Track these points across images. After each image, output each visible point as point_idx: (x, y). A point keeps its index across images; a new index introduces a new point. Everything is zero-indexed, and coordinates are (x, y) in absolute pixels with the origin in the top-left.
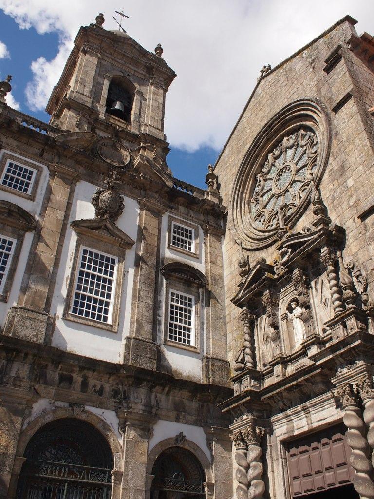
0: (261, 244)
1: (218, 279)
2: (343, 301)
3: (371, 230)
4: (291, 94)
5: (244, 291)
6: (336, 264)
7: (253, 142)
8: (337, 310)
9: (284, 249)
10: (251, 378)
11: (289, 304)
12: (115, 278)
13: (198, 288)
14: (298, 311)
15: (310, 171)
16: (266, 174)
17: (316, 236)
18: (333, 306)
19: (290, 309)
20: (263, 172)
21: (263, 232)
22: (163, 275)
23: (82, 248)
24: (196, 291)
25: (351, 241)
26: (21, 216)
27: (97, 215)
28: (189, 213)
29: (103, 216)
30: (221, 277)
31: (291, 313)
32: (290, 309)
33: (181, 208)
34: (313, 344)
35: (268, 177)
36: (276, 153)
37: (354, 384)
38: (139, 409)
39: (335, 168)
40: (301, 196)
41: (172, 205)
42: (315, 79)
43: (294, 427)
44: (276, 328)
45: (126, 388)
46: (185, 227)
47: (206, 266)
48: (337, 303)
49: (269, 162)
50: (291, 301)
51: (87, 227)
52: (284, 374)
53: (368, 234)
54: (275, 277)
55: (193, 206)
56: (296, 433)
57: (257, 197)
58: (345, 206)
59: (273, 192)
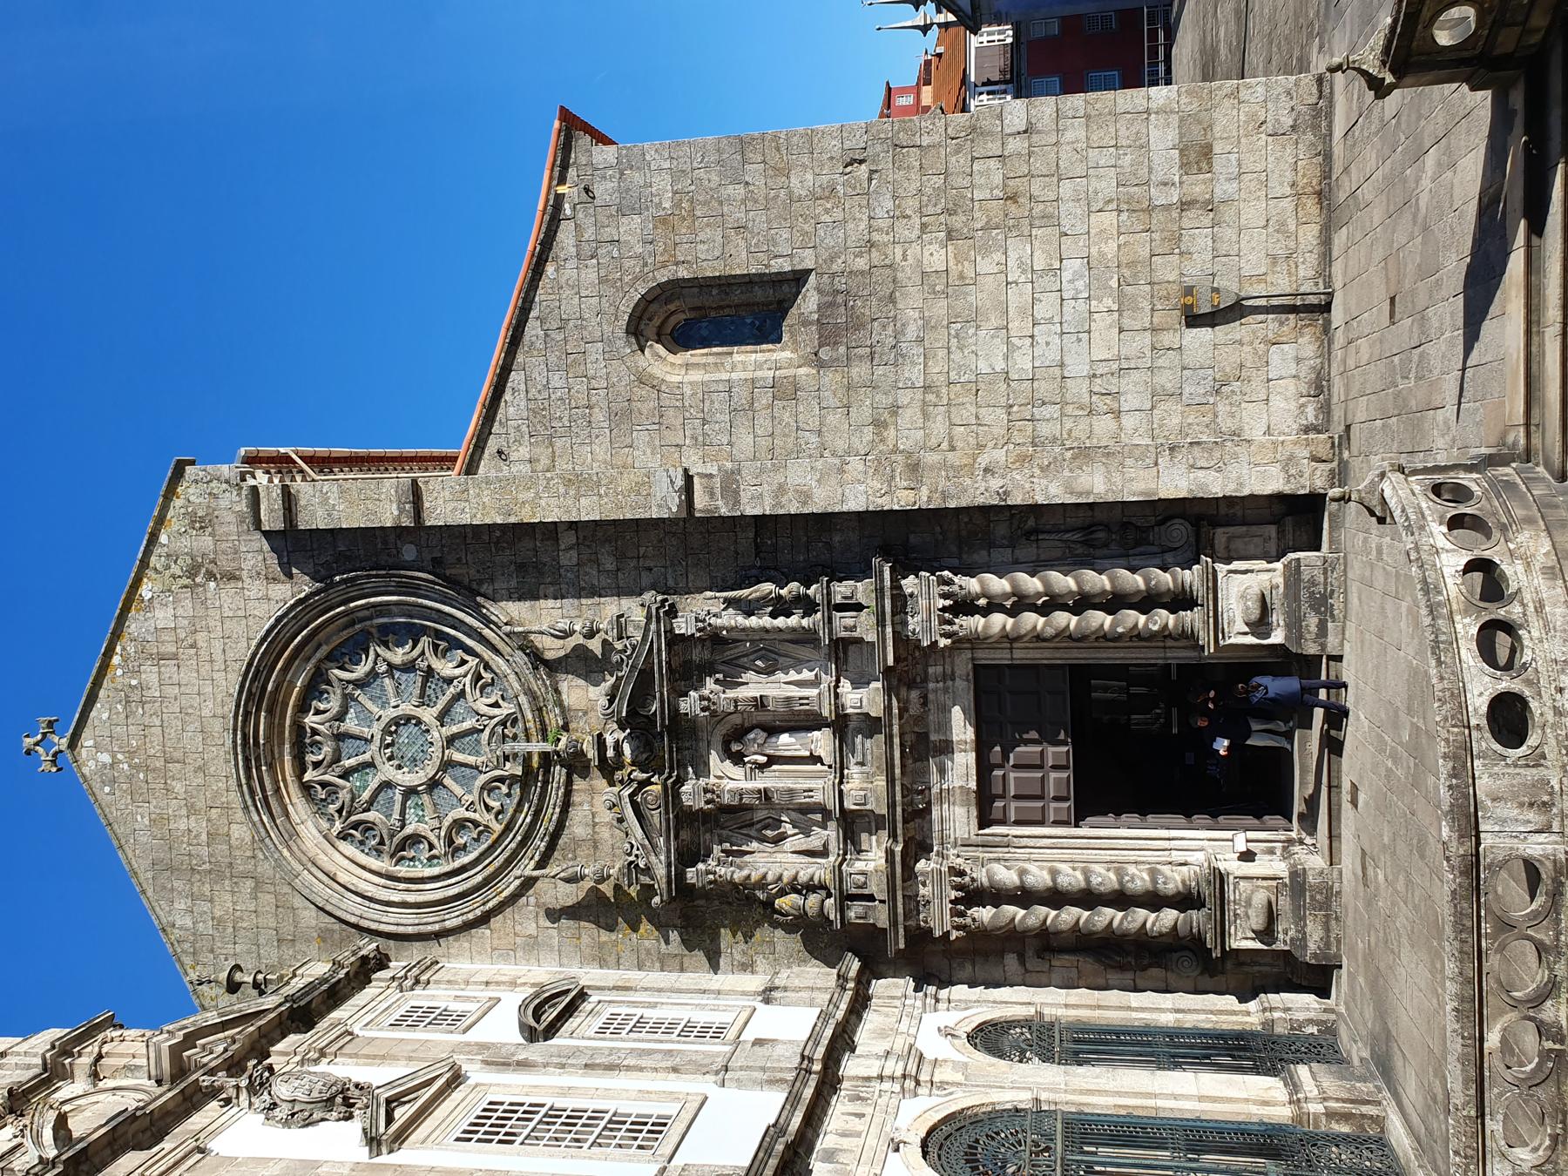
3: (720, 503)
4: (218, 656)
7: (246, 808)
15: (450, 665)
16: (353, 800)
17: (653, 627)
19: (738, 759)
20: (340, 811)
35: (366, 795)
36: (321, 757)
37: (941, 603)
39: (513, 583)
40: (491, 701)
42: (248, 581)
43: (961, 787)
49: (324, 785)
55: (341, 993)
56: (973, 785)
57: (396, 840)
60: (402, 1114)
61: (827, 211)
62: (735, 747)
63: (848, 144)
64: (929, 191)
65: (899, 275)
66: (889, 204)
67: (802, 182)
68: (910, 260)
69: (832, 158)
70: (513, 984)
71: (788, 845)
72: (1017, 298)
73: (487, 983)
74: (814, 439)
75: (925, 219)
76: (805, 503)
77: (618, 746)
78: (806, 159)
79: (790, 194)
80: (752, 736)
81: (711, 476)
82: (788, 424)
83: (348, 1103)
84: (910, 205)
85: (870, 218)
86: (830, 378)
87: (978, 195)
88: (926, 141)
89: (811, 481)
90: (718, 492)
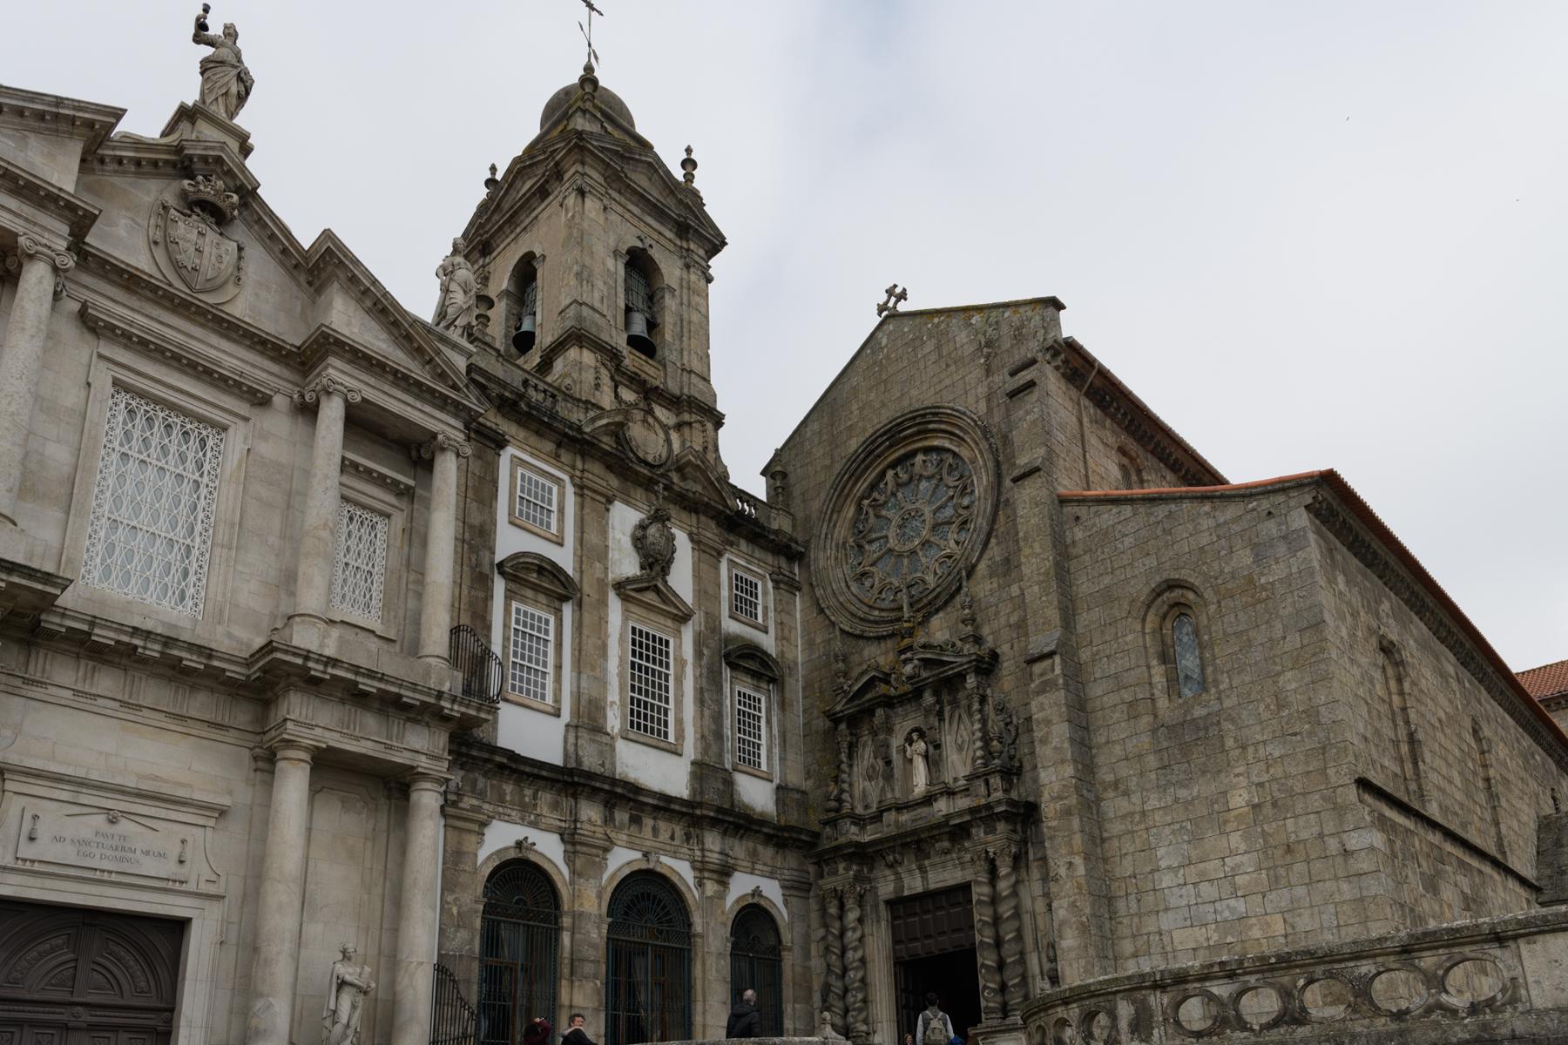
0: (871, 631)
1: (792, 668)
2: (989, 754)
3: (1037, 682)
5: (846, 703)
6: (983, 700)
8: (979, 761)
9: (909, 655)
10: (853, 823)
11: (910, 734)
12: (671, 672)
13: (769, 682)
14: (921, 746)
17: (965, 660)
18: (971, 754)
19: (910, 741)
21: (870, 607)
22: (727, 664)
23: (631, 624)
24: (764, 685)
25: (1004, 673)
26: (554, 576)
27: (642, 568)
28: (753, 551)
29: (651, 569)
30: (796, 664)
31: (910, 745)
32: (910, 741)
33: (743, 545)
34: (941, 794)
38: (714, 858)
41: (732, 538)
44: (888, 763)
45: (698, 831)
46: (750, 578)
47: (777, 645)
48: (979, 753)
50: (914, 730)
51: (633, 590)
52: (897, 821)
53: (1033, 686)
54: (892, 692)
58: (1003, 621)
59: (892, 543)
60: (650, 597)
61: (1267, 707)
62: (915, 735)
63: (1322, 709)
64: (1290, 782)
65: (1223, 775)
66: (1277, 754)
67: (1290, 681)
68: (1235, 780)
69: (1310, 699)
70: (782, 638)
71: (867, 783)
72: (1212, 867)
73: (782, 623)
74: (1103, 740)
75: (1267, 785)
76: (1041, 741)
77: (911, 660)
78: (1308, 679)
79: (1278, 674)
80: (923, 744)
81: (1053, 670)
82: (1111, 717)
83: (651, 566)
84: (1277, 771)
85: (1264, 742)
86: (1146, 739)
87: (1290, 822)
88: (1331, 772)
89: (1055, 742)
90: (1044, 679)
